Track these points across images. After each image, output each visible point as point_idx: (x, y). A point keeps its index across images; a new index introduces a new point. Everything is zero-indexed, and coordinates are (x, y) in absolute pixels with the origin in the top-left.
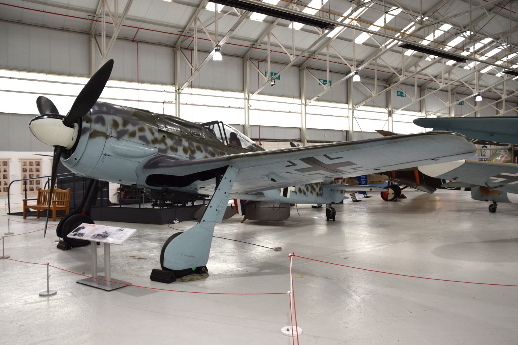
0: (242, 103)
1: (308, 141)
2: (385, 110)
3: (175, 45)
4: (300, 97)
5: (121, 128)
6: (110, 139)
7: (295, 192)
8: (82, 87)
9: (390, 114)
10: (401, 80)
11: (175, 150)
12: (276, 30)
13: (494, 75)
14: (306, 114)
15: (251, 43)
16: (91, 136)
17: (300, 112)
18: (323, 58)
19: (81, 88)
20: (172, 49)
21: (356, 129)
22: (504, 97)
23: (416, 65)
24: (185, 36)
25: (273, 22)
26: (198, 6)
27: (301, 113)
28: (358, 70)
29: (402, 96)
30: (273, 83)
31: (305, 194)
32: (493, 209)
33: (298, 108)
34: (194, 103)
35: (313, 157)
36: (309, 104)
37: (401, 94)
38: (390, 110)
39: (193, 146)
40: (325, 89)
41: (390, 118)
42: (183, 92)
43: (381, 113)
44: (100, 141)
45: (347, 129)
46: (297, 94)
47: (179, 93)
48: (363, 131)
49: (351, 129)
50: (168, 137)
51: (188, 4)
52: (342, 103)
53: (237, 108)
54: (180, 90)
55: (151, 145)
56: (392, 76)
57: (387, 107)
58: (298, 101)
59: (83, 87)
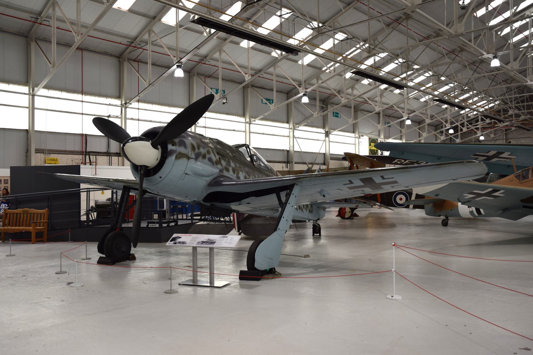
4: (244, 115)
5: (197, 151)
6: (191, 160)
7: (296, 208)
9: (327, 134)
10: (343, 102)
11: (228, 170)
12: (228, 47)
13: (419, 100)
14: (250, 132)
15: (200, 58)
16: (177, 158)
18: (269, 77)
20: (117, 59)
21: (297, 149)
22: (428, 121)
23: (353, 88)
24: (135, 47)
25: (225, 40)
26: (154, 18)
28: (306, 92)
29: (337, 117)
30: (225, 101)
31: (302, 210)
32: (445, 224)
34: (140, 118)
35: (371, 178)
36: (254, 122)
37: (336, 115)
39: (230, 165)
40: (272, 108)
41: (327, 139)
42: (130, 106)
43: (318, 133)
44: (184, 161)
45: (288, 149)
46: (241, 112)
47: (126, 108)
49: (292, 149)
50: (223, 159)
51: (144, 15)
52: (283, 122)
54: (128, 105)
55: (215, 165)
56: (329, 97)
57: (324, 127)
58: (242, 119)
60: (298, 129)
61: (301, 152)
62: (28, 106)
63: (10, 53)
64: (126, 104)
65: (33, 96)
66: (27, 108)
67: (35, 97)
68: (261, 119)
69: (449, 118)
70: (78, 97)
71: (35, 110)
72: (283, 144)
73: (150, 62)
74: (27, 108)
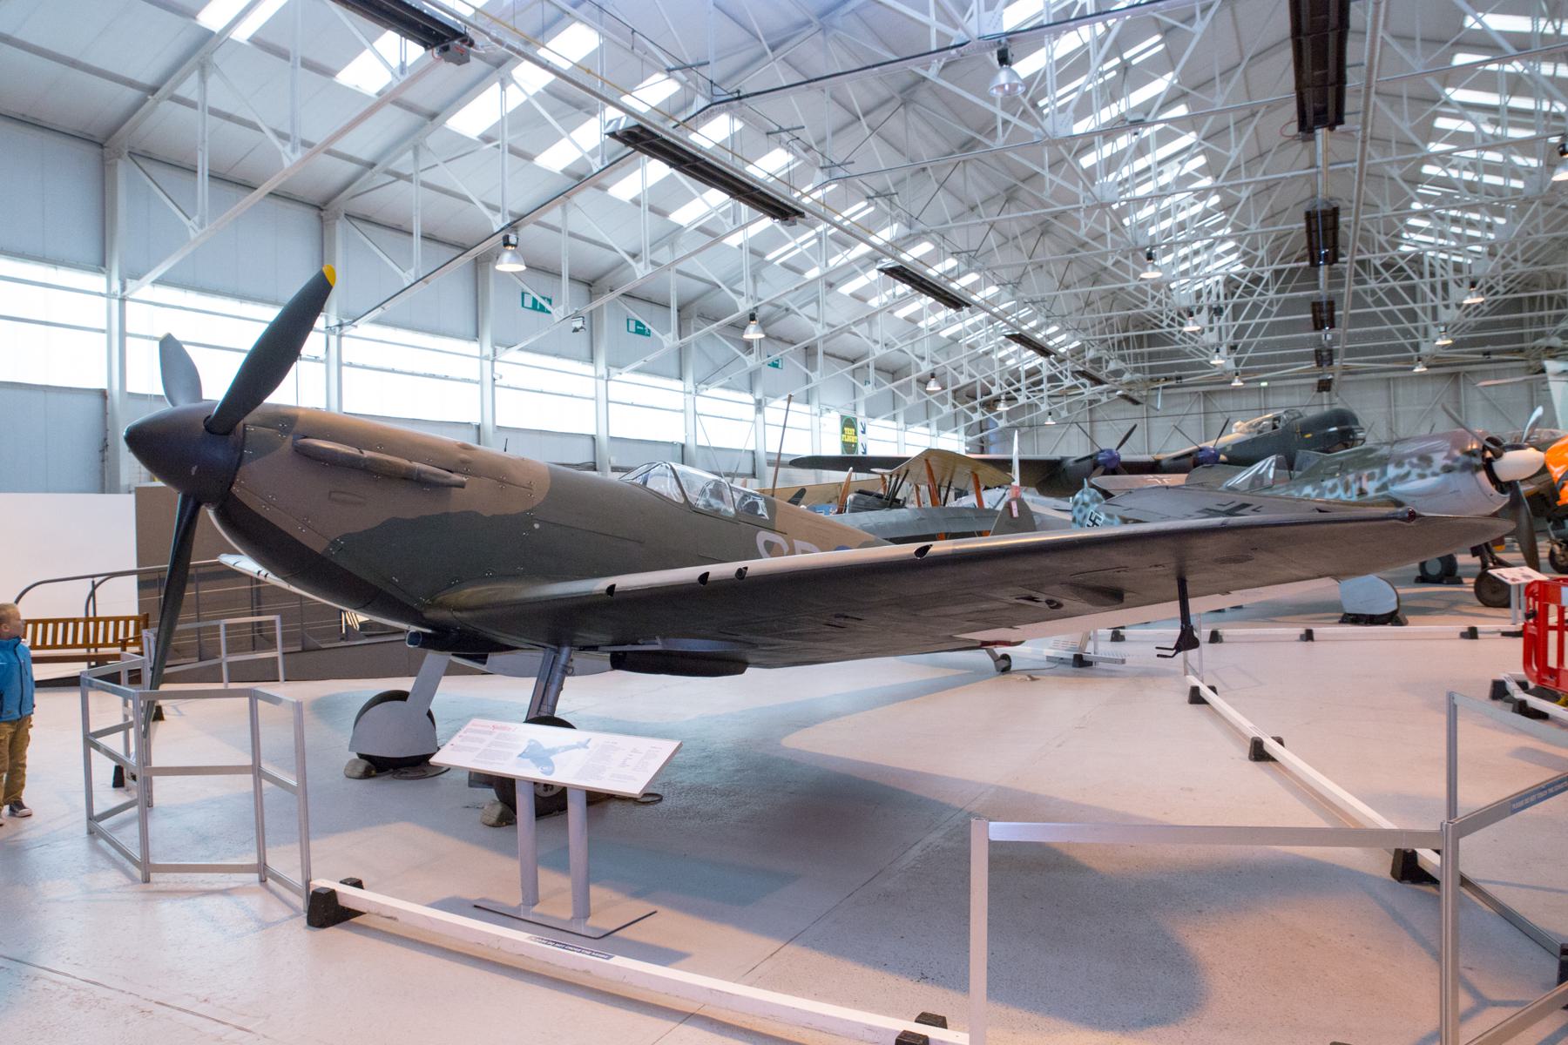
0: (471, 369)
1: (615, 469)
2: (749, 398)
3: (326, 203)
8: (263, 328)
9: (759, 406)
19: (259, 331)
20: (316, 212)
21: (702, 442)
26: (433, 116)
27: (595, 399)
33: (587, 387)
36: (618, 377)
38: (758, 397)
40: (666, 344)
47: (340, 336)
53: (425, 375)
57: (751, 391)
59: (266, 326)
61: (708, 448)
62: (104, 327)
63: (61, 185)
64: (341, 325)
65: (123, 300)
68: (638, 371)
69: (996, 377)
71: (128, 339)
72: (670, 430)
73: (417, 231)
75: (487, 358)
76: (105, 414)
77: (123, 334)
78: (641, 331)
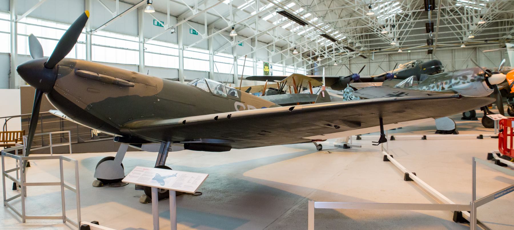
1: (185, 81)
2: (232, 56)
8: (64, 32)
9: (235, 59)
17: (178, 55)
19: (63, 33)
21: (216, 71)
27: (179, 56)
36: (187, 49)
40: (203, 38)
41: (235, 62)
42: (96, 33)
47: (91, 35)
48: (219, 72)
53: (120, 48)
54: (93, 32)
57: (233, 53)
59: (65, 32)
60: (217, 54)
65: (16, 22)
66: (9, 33)
67: (18, 24)
68: (193, 47)
69: (317, 49)
70: (40, 22)
71: (18, 36)
72: (205, 67)
74: (9, 33)
75: (141, 42)
76: (10, 61)
77: (16, 34)
78: (195, 33)
